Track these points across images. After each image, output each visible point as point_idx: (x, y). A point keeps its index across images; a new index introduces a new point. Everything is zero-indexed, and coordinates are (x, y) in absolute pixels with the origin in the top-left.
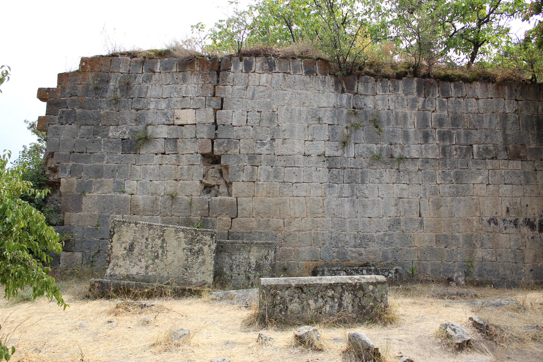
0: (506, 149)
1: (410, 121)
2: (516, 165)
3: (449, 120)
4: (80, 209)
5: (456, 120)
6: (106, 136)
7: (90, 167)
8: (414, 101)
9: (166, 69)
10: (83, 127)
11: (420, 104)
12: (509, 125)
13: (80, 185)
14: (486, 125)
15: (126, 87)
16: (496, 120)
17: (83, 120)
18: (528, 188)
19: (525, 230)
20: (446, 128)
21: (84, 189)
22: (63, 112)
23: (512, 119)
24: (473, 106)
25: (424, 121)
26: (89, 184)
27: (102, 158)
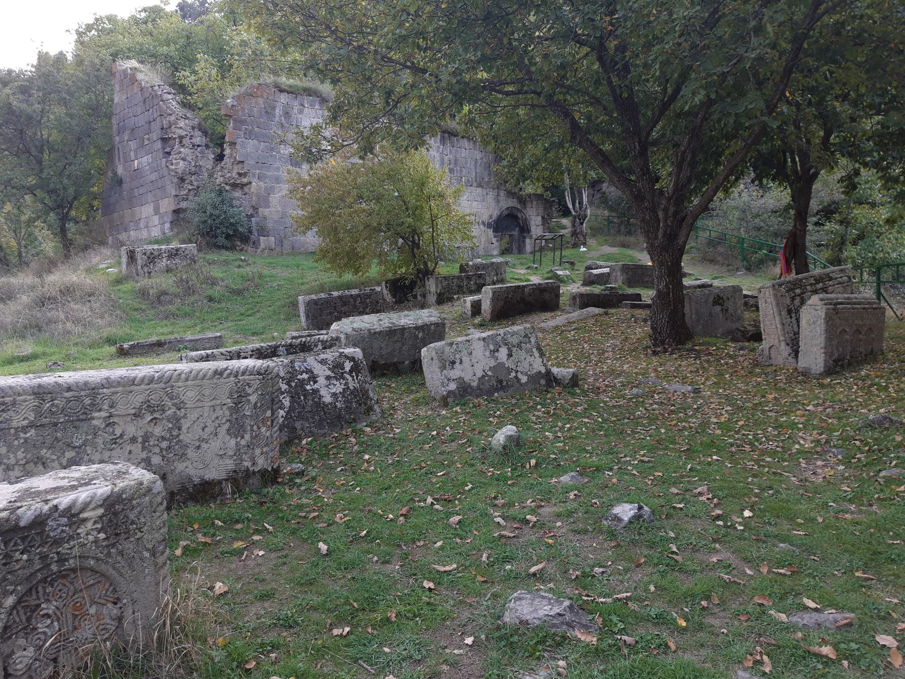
0: (476, 181)
1: (436, 160)
2: (479, 190)
3: (453, 161)
4: (269, 207)
5: (456, 161)
6: (279, 152)
7: (271, 175)
8: (439, 147)
9: (311, 105)
10: (262, 143)
11: (441, 150)
12: (478, 167)
13: (266, 188)
14: (469, 166)
15: (287, 114)
16: (473, 163)
17: (260, 138)
18: (484, 203)
19: (482, 227)
20: (451, 166)
21: (270, 191)
22: (246, 129)
23: (479, 163)
24: (464, 153)
25: (442, 160)
26: (272, 188)
27: (278, 169)
